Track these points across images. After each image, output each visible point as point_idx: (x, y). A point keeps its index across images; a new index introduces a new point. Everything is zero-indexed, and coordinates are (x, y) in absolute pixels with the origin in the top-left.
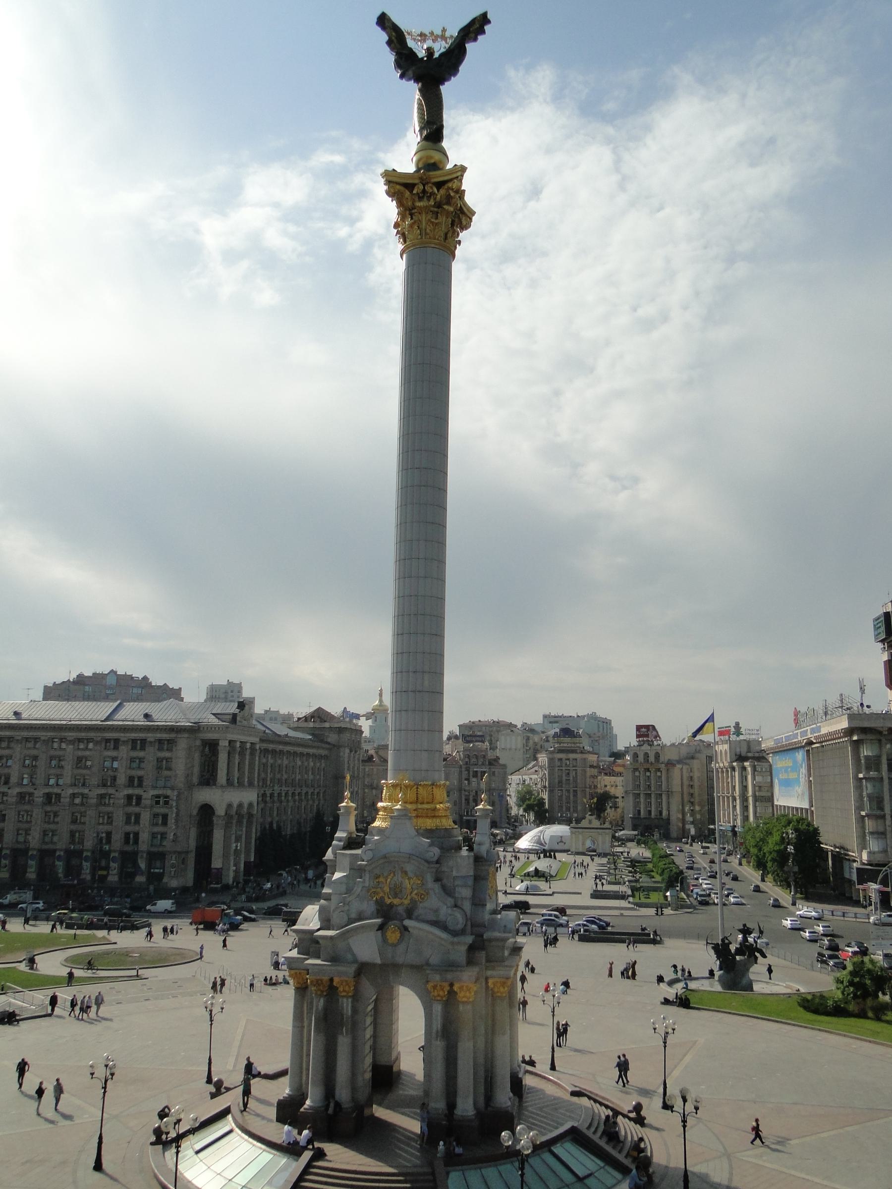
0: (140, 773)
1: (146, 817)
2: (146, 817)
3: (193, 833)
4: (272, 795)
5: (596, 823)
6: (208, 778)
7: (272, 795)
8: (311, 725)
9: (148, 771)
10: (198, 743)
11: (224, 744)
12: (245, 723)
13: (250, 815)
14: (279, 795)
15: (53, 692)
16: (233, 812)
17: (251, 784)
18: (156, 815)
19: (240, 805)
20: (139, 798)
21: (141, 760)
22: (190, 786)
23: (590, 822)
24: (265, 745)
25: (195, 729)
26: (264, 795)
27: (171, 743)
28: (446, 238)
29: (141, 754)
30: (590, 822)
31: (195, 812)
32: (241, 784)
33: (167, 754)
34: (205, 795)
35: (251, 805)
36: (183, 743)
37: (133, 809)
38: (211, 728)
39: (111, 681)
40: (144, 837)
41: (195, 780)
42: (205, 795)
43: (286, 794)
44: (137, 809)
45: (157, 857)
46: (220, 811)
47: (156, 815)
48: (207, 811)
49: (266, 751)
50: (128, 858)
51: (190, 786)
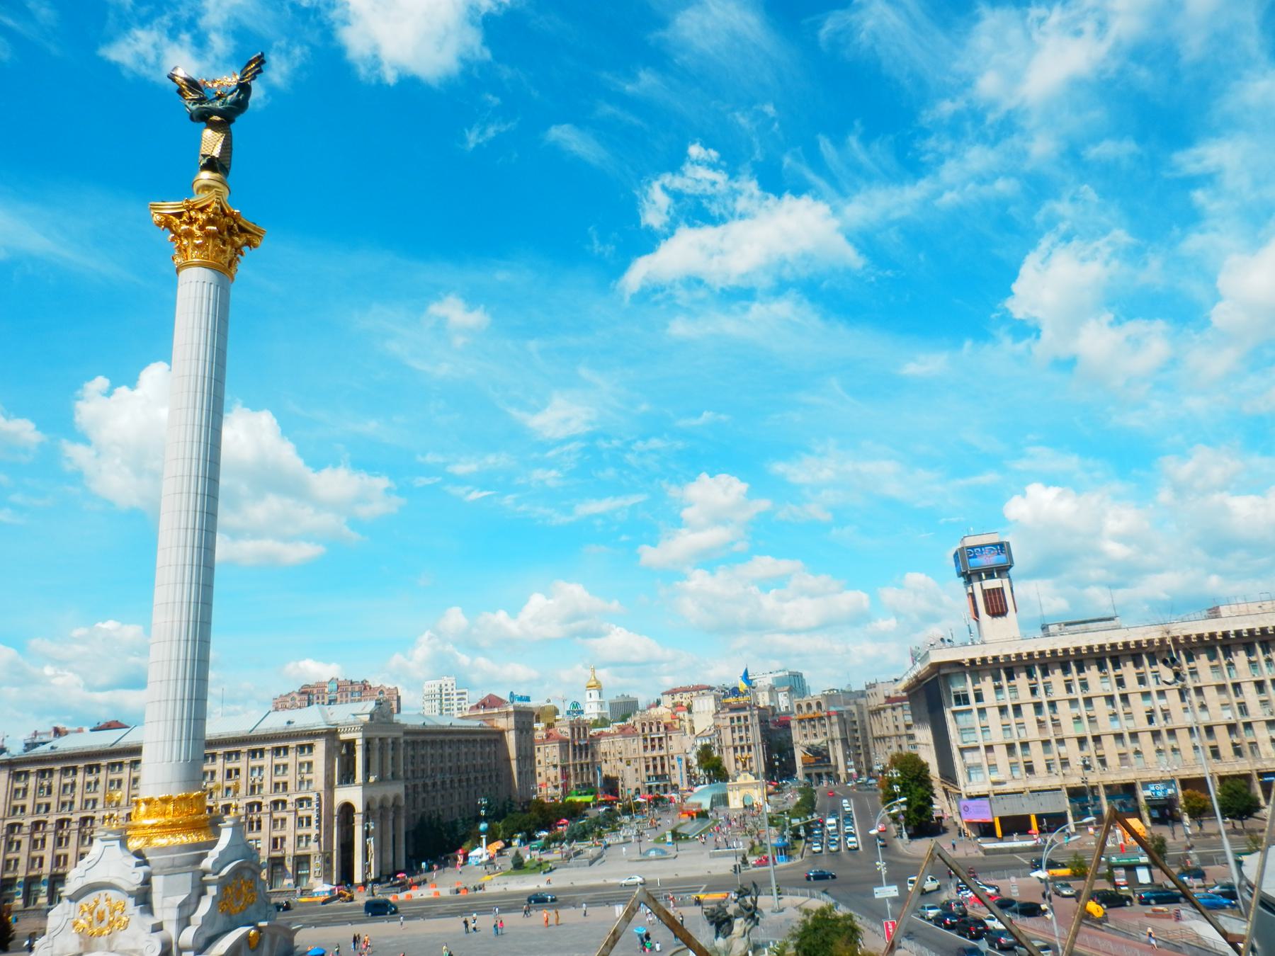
0: (284, 779)
1: (291, 820)
4: (434, 784)
5: (751, 779)
6: (348, 777)
7: (434, 784)
8: (481, 712)
9: (290, 777)
11: (359, 742)
13: (396, 806)
14: (443, 783)
15: (281, 704)
16: (375, 806)
17: (395, 776)
19: (384, 799)
20: (284, 802)
21: (285, 766)
22: (330, 787)
23: (745, 778)
24: (409, 738)
25: (331, 734)
26: (415, 786)
27: (311, 747)
28: (230, 265)
29: (284, 761)
30: (745, 778)
33: (309, 758)
35: (396, 798)
38: (349, 727)
43: (452, 781)
44: (283, 815)
46: (359, 807)
47: (300, 820)
49: (414, 743)
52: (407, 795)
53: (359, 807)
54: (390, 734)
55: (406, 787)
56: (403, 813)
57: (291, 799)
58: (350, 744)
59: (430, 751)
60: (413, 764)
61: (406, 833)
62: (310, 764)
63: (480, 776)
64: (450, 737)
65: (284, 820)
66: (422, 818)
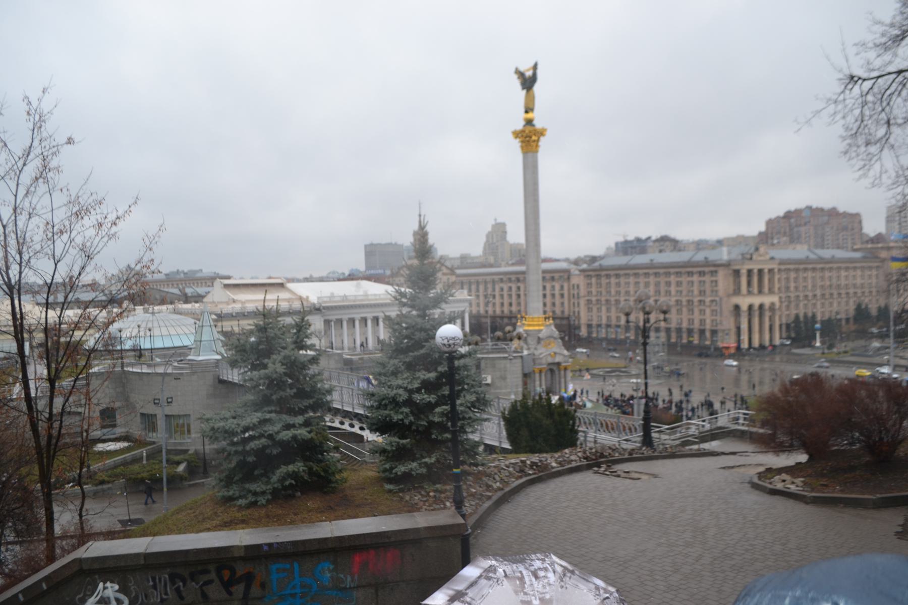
1: (708, 311)
2: (708, 311)
3: (732, 320)
6: (737, 292)
7: (815, 296)
8: (870, 246)
9: (708, 287)
10: (731, 272)
11: (744, 272)
12: (762, 258)
17: (771, 291)
18: (713, 311)
19: (761, 307)
21: (704, 282)
25: (727, 265)
27: (716, 272)
31: (732, 309)
32: (760, 292)
34: (736, 300)
35: (773, 304)
36: (721, 273)
37: (702, 307)
39: (806, 214)
40: (708, 321)
41: (731, 291)
42: (736, 300)
45: (714, 332)
46: (744, 308)
47: (713, 311)
48: (737, 308)
50: (702, 332)
51: (729, 296)
52: (781, 302)
53: (744, 308)
54: (766, 267)
55: (780, 298)
56: (778, 313)
57: (708, 300)
58: (737, 273)
59: (810, 274)
60: (795, 282)
61: (781, 326)
62: (716, 282)
63: (859, 291)
64: (831, 265)
65: (704, 311)
66: (797, 317)
